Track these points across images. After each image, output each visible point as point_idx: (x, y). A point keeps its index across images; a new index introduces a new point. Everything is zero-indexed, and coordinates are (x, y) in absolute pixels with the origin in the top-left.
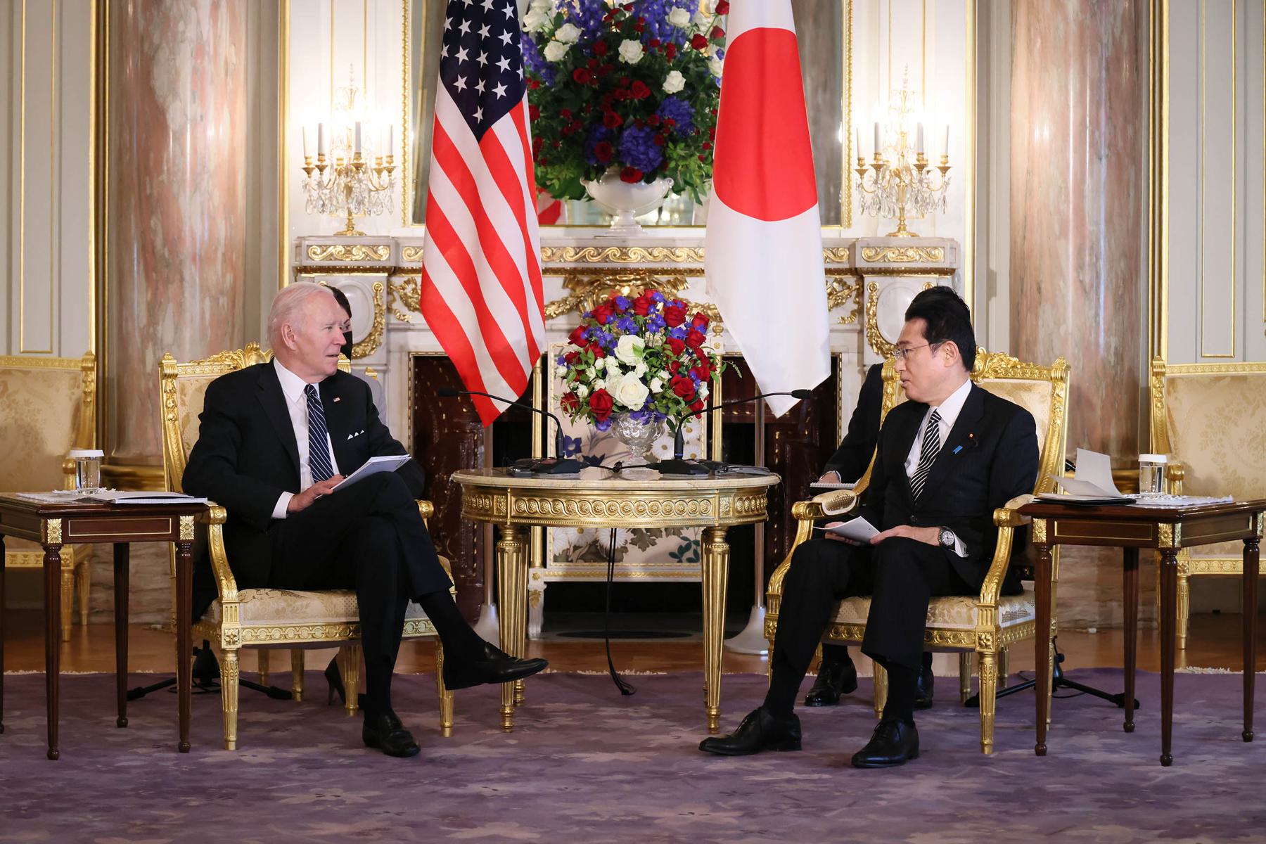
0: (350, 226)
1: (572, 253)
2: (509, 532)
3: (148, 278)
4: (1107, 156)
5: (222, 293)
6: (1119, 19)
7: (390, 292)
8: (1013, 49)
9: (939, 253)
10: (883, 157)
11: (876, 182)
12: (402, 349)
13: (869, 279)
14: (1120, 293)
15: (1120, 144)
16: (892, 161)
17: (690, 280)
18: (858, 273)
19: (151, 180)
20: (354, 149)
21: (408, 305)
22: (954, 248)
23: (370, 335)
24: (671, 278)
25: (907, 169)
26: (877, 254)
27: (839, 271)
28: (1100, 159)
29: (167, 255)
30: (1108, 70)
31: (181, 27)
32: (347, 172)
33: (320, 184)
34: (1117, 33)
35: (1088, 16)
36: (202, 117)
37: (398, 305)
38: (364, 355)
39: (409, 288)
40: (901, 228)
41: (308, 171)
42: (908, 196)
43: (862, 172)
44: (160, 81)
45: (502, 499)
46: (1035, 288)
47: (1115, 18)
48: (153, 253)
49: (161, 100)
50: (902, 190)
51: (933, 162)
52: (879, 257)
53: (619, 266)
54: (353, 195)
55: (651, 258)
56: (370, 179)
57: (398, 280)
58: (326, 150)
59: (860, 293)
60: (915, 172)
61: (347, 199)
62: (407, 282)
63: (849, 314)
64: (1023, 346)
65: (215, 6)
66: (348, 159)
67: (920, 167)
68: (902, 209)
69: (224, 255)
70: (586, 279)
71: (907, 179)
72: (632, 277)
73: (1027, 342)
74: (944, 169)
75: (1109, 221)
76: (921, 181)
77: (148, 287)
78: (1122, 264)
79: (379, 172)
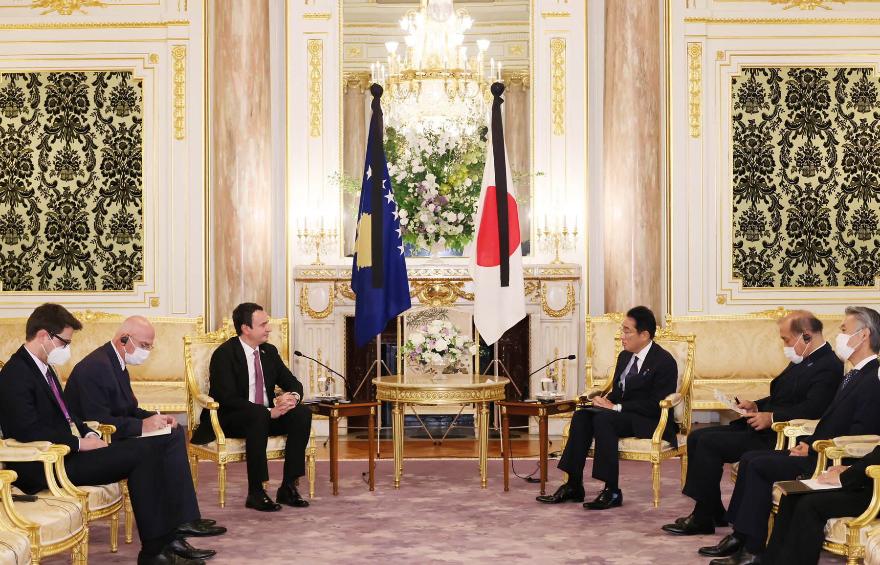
0: (318, 260)
1: (414, 272)
2: (397, 406)
3: (229, 282)
4: (646, 226)
5: (262, 288)
6: (650, 166)
7: (336, 289)
8: (604, 179)
9: (573, 271)
10: (549, 229)
11: (546, 240)
12: (341, 313)
13: (543, 283)
14: (652, 285)
15: (652, 221)
16: (552, 230)
17: (465, 283)
18: (537, 279)
19: (231, 241)
20: (320, 226)
21: (343, 295)
22: (580, 268)
23: (328, 308)
24: (457, 282)
25: (560, 235)
26: (546, 271)
27: (529, 279)
28: (643, 227)
29: (238, 272)
30: (646, 189)
31: (243, 174)
32: (316, 237)
33: (305, 243)
34: (650, 172)
35: (637, 165)
36: (252, 213)
37: (339, 295)
38: (324, 317)
39: (344, 288)
40: (557, 259)
41: (299, 236)
42: (559, 245)
43: (539, 235)
44: (235, 196)
45: (394, 392)
46: (615, 284)
47: (649, 166)
48: (232, 272)
49: (235, 205)
50: (557, 242)
51: (570, 231)
52: (546, 273)
53: (434, 277)
54: (320, 247)
55: (449, 274)
56: (327, 240)
57: (339, 284)
58: (308, 228)
59: (539, 287)
60: (563, 235)
61: (317, 249)
62: (343, 285)
63: (534, 297)
64: (610, 308)
65: (258, 164)
66: (317, 232)
67: (565, 233)
68: (557, 252)
69: (263, 272)
70: (421, 283)
71: (558, 237)
72: (440, 282)
73: (612, 307)
74: (575, 234)
75: (647, 254)
76: (565, 239)
77: (230, 287)
78: (653, 273)
79: (330, 236)
